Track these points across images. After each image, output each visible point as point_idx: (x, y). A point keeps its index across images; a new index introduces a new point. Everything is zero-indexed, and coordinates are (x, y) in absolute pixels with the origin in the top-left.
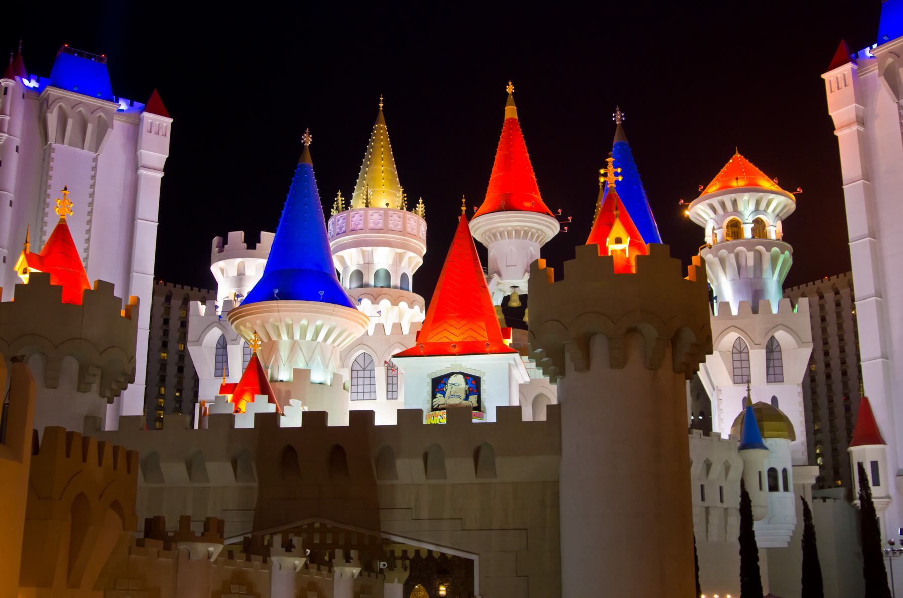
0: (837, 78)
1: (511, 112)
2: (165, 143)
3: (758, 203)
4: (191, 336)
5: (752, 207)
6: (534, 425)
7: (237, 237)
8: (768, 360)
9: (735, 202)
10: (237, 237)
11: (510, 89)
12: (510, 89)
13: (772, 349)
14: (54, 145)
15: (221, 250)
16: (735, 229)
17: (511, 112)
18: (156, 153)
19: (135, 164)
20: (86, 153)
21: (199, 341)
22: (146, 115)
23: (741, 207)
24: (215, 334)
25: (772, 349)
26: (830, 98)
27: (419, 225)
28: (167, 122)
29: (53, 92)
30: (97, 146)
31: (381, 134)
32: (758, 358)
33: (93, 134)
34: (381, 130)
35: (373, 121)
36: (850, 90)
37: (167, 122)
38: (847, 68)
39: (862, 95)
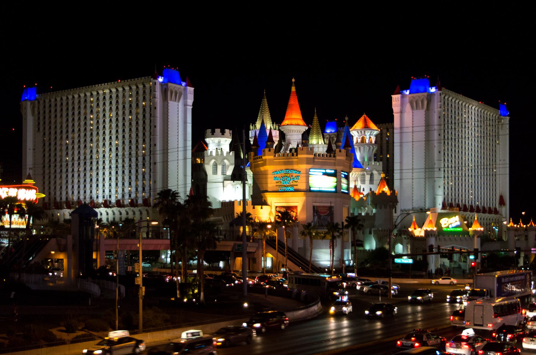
0: (396, 99)
1: (293, 89)
2: (192, 96)
3: (371, 132)
4: (206, 161)
5: (369, 134)
6: (371, 216)
7: (218, 131)
8: (371, 178)
9: (364, 132)
10: (218, 131)
11: (293, 80)
12: (293, 80)
13: (372, 175)
14: (169, 102)
15: (213, 134)
16: (363, 140)
17: (293, 89)
18: (190, 101)
19: (185, 105)
20: (176, 103)
21: (208, 164)
22: (188, 88)
23: (366, 133)
24: (213, 161)
25: (372, 175)
26: (393, 103)
27: (276, 133)
28: (193, 89)
29: (170, 84)
30: (179, 102)
31: (265, 101)
32: (368, 177)
33: (177, 96)
34: (265, 101)
35: (263, 98)
36: (399, 103)
37: (193, 89)
38: (399, 96)
39: (402, 105)
